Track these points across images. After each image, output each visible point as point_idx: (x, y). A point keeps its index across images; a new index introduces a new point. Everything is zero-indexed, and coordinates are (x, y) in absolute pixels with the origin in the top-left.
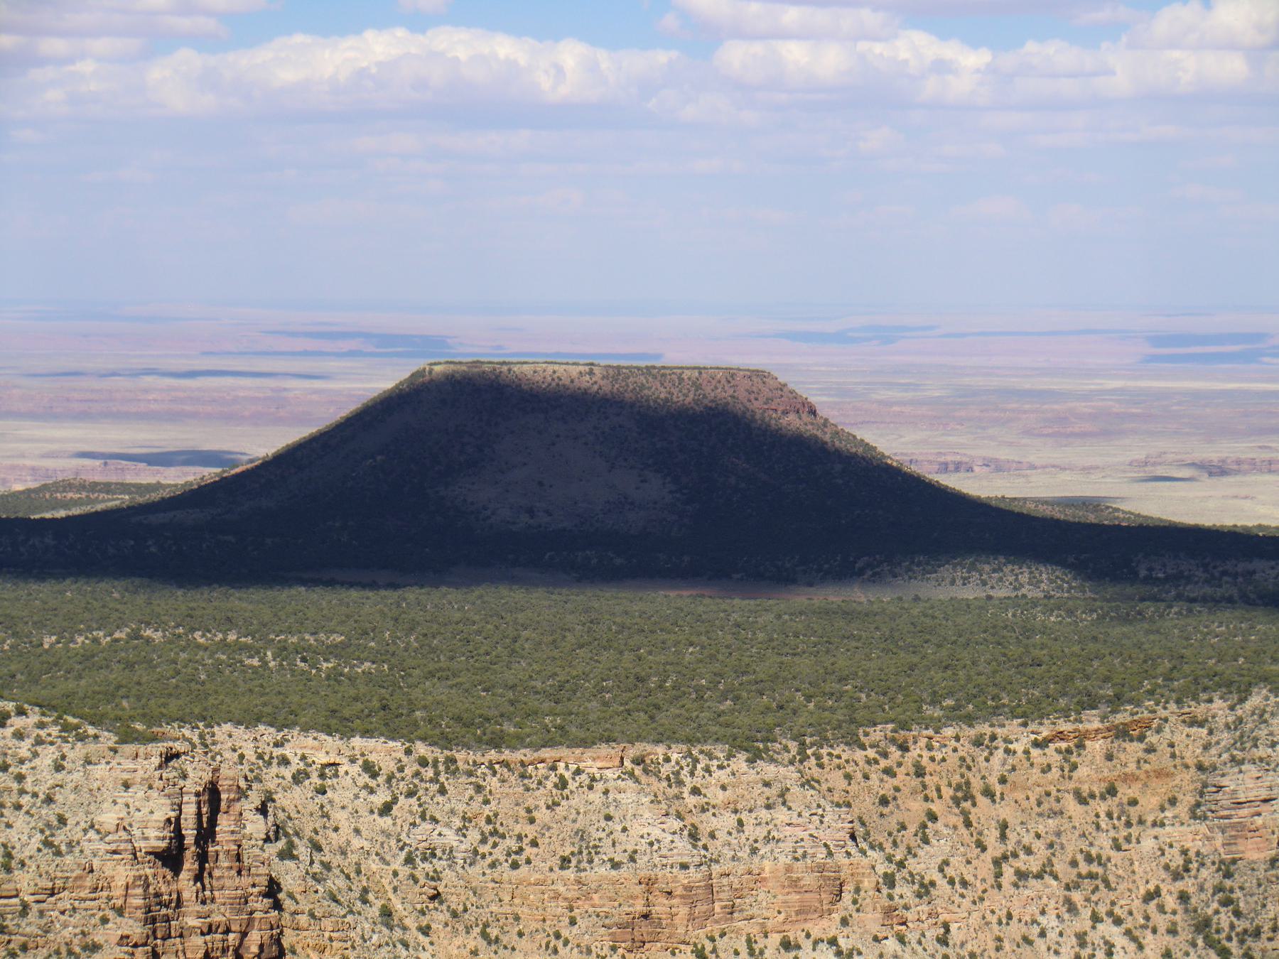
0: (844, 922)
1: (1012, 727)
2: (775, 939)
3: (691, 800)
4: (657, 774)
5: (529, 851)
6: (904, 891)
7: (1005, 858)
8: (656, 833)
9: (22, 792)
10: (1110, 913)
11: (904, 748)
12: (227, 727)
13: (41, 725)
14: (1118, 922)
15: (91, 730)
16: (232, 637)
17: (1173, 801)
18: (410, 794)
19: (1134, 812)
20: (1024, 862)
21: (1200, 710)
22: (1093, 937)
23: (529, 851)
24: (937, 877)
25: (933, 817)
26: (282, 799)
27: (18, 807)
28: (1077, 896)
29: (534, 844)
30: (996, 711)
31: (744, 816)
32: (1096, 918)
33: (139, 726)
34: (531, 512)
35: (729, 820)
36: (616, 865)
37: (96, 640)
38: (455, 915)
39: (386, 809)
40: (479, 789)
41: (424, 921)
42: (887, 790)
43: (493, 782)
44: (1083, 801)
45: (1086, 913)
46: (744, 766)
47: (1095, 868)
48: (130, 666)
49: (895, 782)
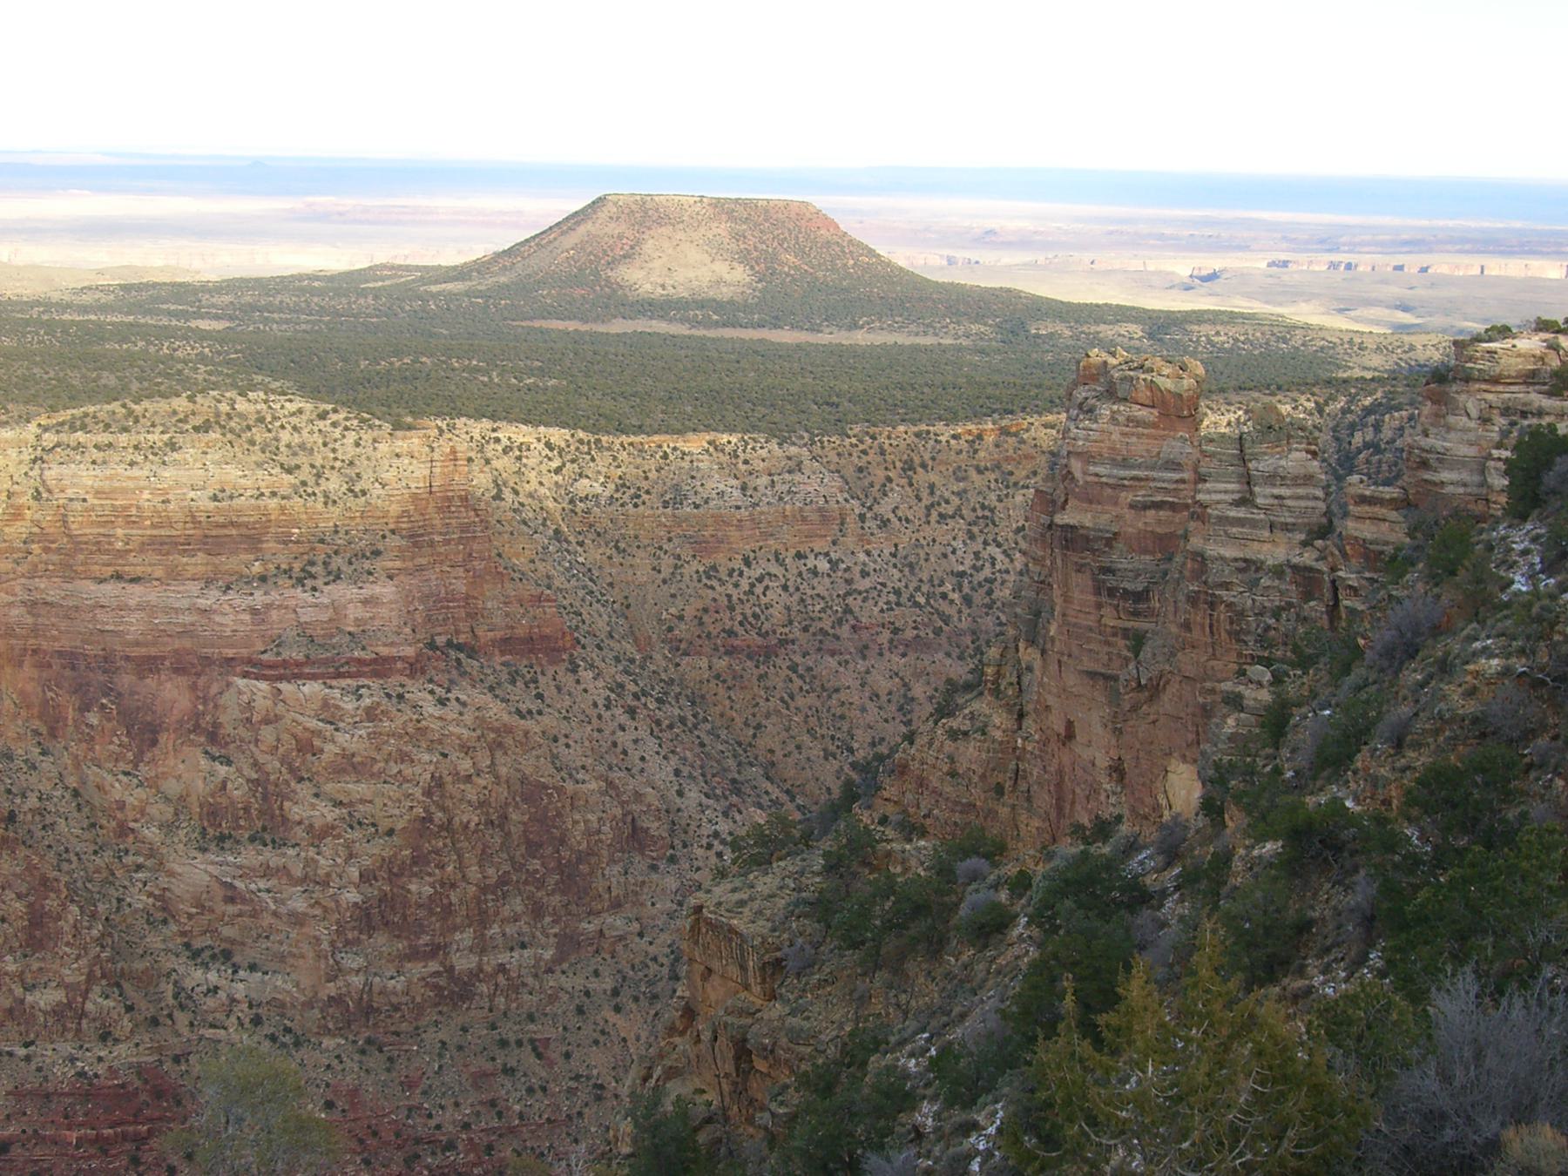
0: (834, 543)
1: (939, 427)
2: (793, 552)
3: (743, 467)
4: (723, 451)
5: (645, 497)
7: (932, 505)
8: (721, 487)
9: (336, 459)
10: (994, 540)
12: (464, 419)
13: (347, 419)
14: (999, 545)
15: (377, 422)
17: (1035, 473)
18: (573, 461)
19: (1012, 479)
20: (944, 508)
21: (1051, 418)
22: (985, 555)
24: (891, 516)
25: (890, 480)
26: (495, 463)
27: (333, 468)
28: (975, 529)
29: (648, 492)
31: (776, 478)
32: (986, 543)
33: (409, 419)
34: (663, 287)
35: (765, 480)
36: (697, 506)
37: (391, 364)
38: (599, 534)
39: (558, 471)
40: (615, 458)
41: (581, 538)
43: (623, 455)
44: (980, 472)
45: (980, 540)
47: (987, 513)
49: (869, 458)
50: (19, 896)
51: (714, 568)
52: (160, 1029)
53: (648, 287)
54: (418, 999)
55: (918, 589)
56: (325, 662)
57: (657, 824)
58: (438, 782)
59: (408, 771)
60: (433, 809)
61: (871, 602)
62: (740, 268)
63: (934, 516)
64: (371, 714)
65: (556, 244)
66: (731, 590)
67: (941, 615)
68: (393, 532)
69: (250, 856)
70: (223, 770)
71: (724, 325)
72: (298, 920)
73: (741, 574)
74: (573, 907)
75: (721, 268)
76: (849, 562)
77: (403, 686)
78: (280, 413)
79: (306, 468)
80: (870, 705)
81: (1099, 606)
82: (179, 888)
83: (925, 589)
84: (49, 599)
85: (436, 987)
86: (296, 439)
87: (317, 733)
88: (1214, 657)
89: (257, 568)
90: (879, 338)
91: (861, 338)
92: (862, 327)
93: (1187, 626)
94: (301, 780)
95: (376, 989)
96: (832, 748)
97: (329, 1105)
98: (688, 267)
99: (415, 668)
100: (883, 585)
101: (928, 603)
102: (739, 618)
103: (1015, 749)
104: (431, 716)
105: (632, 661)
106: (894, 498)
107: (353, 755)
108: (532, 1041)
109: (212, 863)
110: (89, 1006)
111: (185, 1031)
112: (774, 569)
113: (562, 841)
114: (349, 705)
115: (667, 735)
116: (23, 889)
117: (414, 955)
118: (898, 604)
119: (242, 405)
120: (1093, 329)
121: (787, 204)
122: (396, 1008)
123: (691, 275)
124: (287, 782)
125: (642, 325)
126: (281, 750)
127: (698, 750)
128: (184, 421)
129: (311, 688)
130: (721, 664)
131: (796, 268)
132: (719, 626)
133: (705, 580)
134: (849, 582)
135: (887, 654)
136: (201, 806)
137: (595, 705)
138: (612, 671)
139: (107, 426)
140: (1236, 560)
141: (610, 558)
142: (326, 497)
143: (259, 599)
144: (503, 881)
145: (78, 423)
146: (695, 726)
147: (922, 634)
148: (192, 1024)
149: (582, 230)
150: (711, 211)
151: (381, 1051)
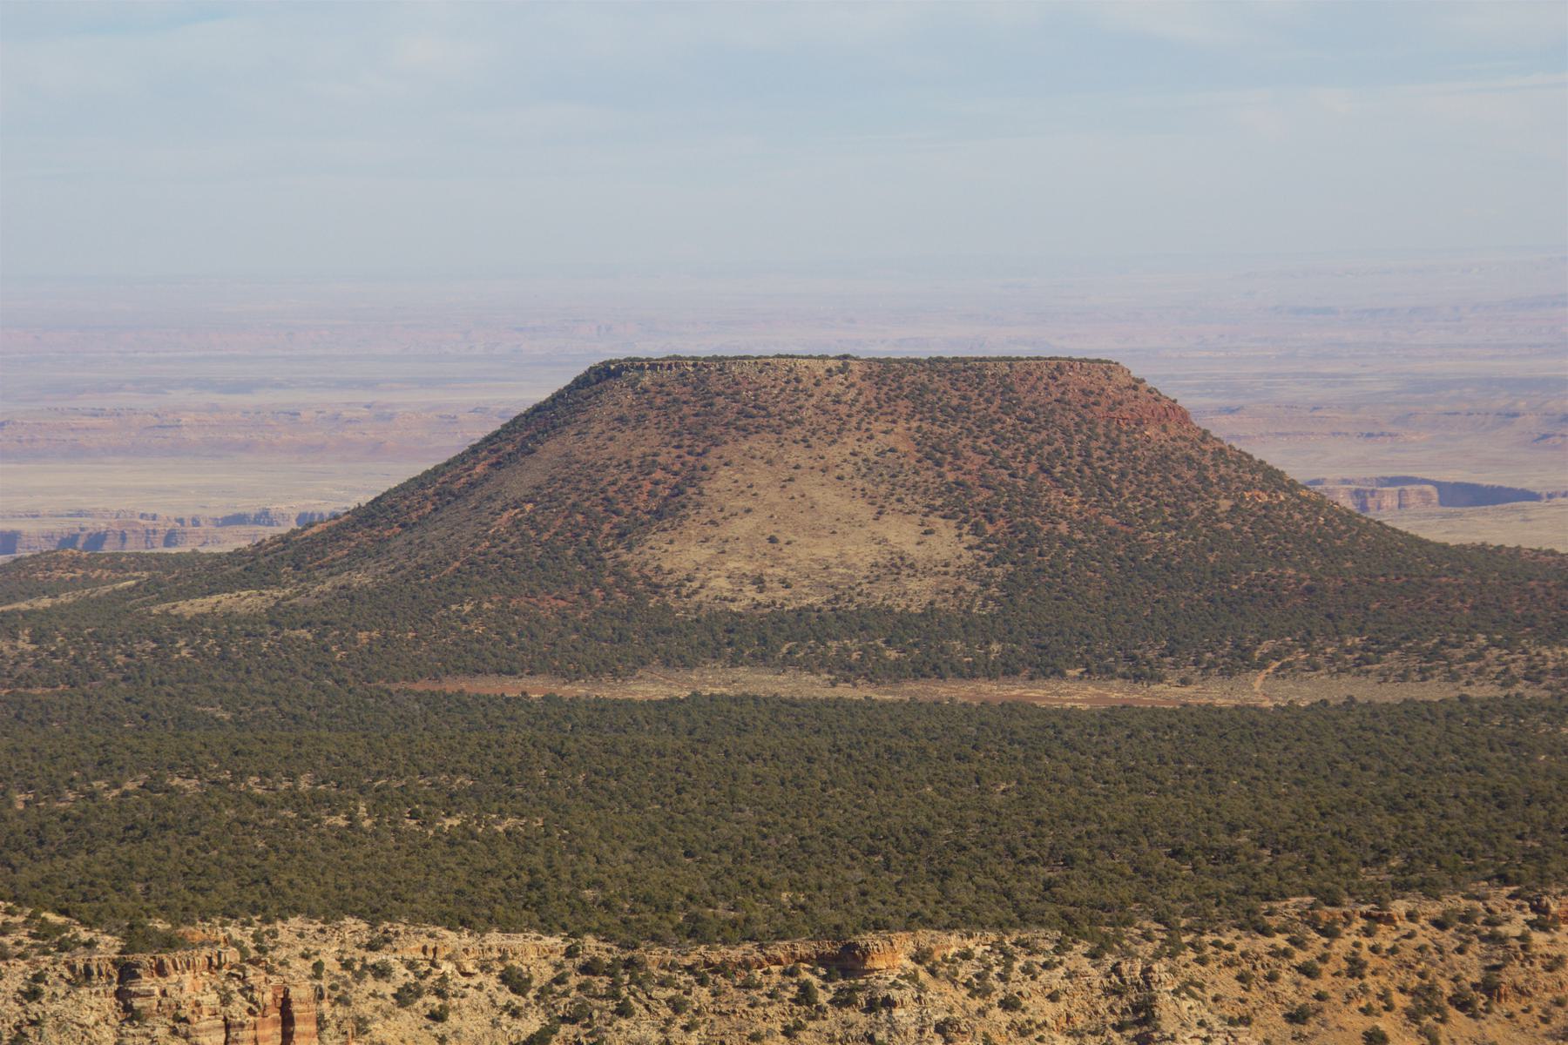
11: (1330, 932)
12: (295, 922)
34: (759, 582)
37: (92, 796)
49: (1321, 985)
53: (721, 584)
62: (946, 531)
65: (488, 489)
71: (919, 673)
75: (902, 534)
91: (1260, 691)
92: (1262, 665)
121: (1059, 367)
123: (826, 550)
149: (551, 449)
150: (870, 394)
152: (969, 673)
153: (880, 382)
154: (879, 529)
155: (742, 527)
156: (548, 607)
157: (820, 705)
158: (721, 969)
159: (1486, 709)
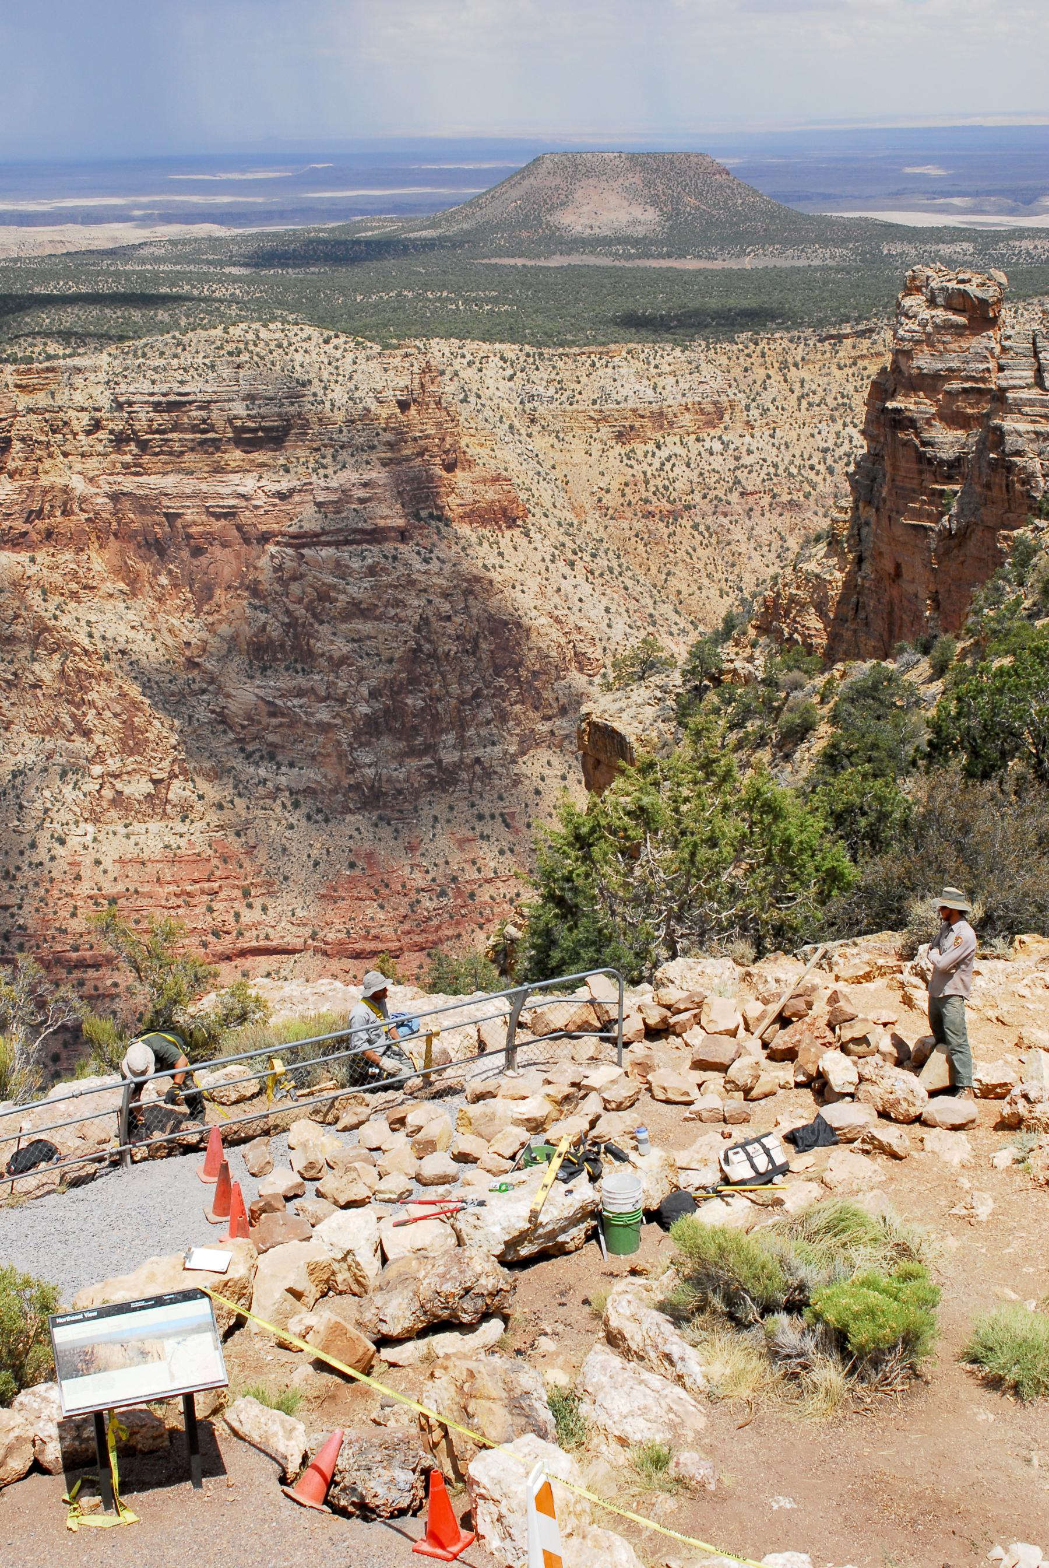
0: (726, 428)
2: (694, 437)
3: (653, 371)
5: (578, 397)
6: (755, 413)
8: (637, 387)
11: (756, 344)
12: (437, 340)
13: (346, 343)
14: (855, 426)
15: (369, 344)
16: (445, 294)
19: (865, 373)
22: (844, 433)
23: (578, 397)
25: (769, 377)
30: (801, 324)
32: (845, 425)
33: (394, 341)
34: (591, 228)
35: (671, 380)
36: (618, 403)
39: (511, 378)
40: (554, 367)
42: (748, 364)
43: (560, 364)
44: (840, 368)
46: (679, 354)
47: (845, 400)
48: (395, 310)
50: (116, 715)
51: (632, 451)
52: (226, 811)
53: (579, 228)
54: (416, 785)
55: (792, 463)
56: (339, 531)
57: (592, 649)
58: (425, 620)
59: (403, 615)
60: (422, 642)
61: (754, 474)
62: (651, 210)
63: (804, 404)
64: (372, 571)
65: (506, 196)
66: (646, 468)
67: (810, 482)
68: (385, 430)
69: (285, 681)
70: (263, 617)
72: (324, 728)
73: (653, 455)
74: (530, 714)
75: (637, 212)
76: (738, 442)
77: (396, 549)
78: (294, 340)
79: (316, 382)
80: (754, 554)
81: (921, 472)
82: (233, 707)
83: (798, 461)
84: (125, 490)
85: (429, 776)
86: (308, 359)
87: (334, 587)
88: (1009, 510)
89: (282, 461)
90: (760, 264)
91: (748, 263)
93: (988, 486)
94: (321, 622)
95: (384, 778)
96: (727, 589)
97: (352, 865)
98: (607, 211)
99: (403, 535)
100: (765, 460)
101: (799, 473)
102: (653, 489)
103: (856, 586)
104: (419, 571)
105: (571, 525)
106: (771, 393)
107: (361, 602)
108: (502, 815)
109: (258, 687)
110: (171, 796)
111: (244, 813)
112: (679, 450)
113: (520, 664)
114: (356, 564)
115: (600, 581)
116: (118, 710)
117: (413, 752)
118: (776, 475)
119: (264, 334)
120: (934, 248)
122: (400, 792)
123: (612, 216)
124: (311, 625)
125: (575, 260)
126: (306, 600)
127: (623, 592)
128: (221, 348)
129: (327, 552)
130: (638, 526)
131: (697, 208)
132: (637, 496)
133: (625, 461)
134: (737, 459)
135: (767, 515)
136: (248, 644)
137: (543, 560)
138: (557, 535)
139: (162, 353)
140: (1028, 432)
141: (552, 446)
142: (333, 405)
143: (284, 486)
144: (477, 694)
145: (140, 353)
146: (620, 574)
147: (795, 498)
148: (248, 808)
151: (389, 824)
152: (661, 256)
153: (631, 160)
154: (630, 210)
155: (585, 209)
156: (524, 234)
157: (606, 269)
158: (566, 355)
159: (816, 269)
